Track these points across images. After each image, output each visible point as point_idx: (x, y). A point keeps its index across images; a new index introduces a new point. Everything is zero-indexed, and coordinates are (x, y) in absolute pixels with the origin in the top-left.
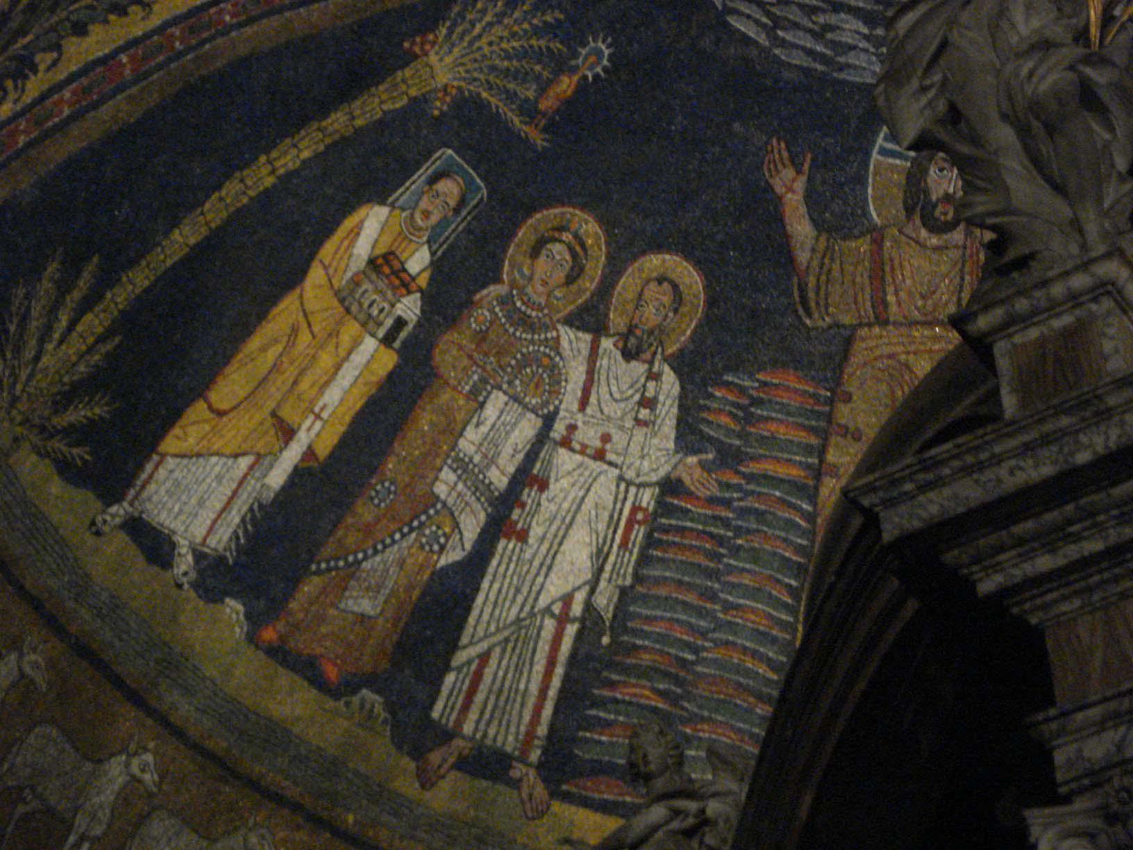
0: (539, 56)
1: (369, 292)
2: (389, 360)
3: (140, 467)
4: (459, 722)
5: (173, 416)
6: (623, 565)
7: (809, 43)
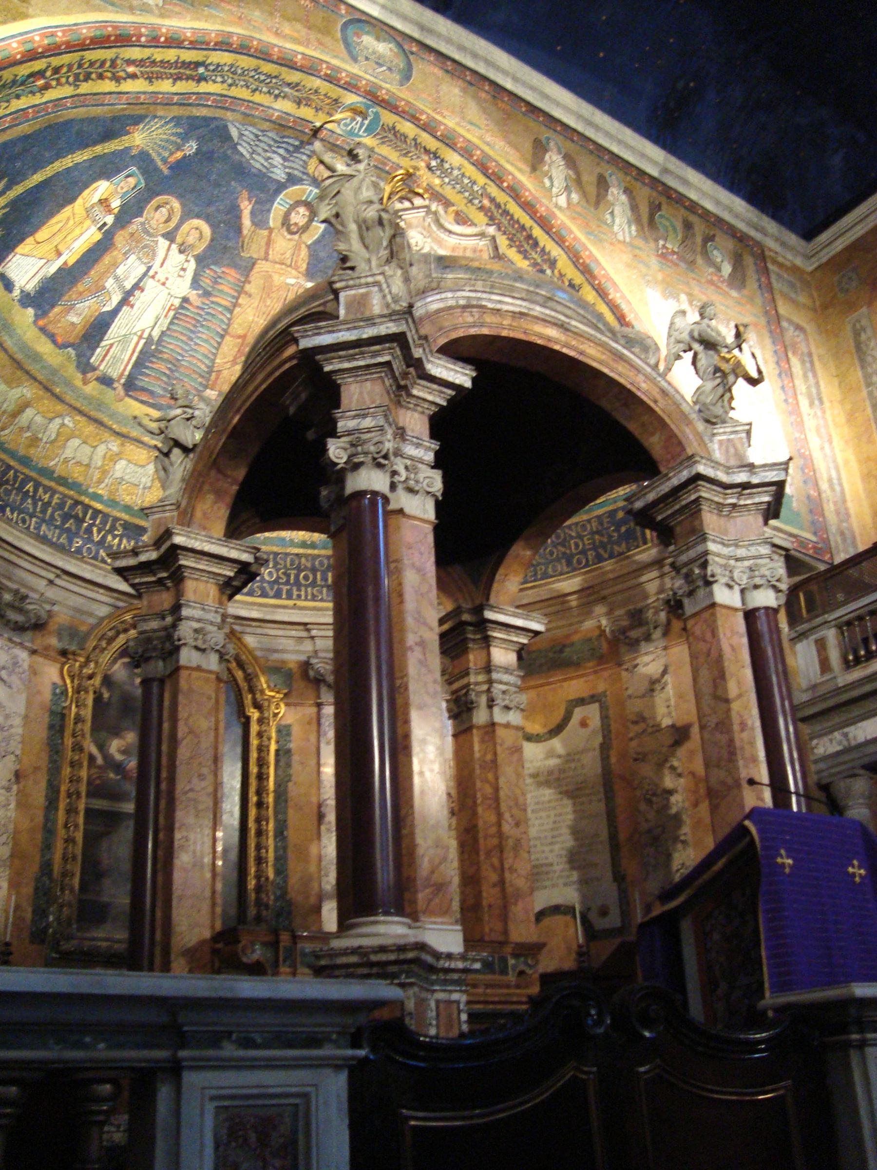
0: (173, 143)
2: (98, 236)
3: (7, 256)
5: (22, 240)
6: (164, 323)
7: (263, 161)
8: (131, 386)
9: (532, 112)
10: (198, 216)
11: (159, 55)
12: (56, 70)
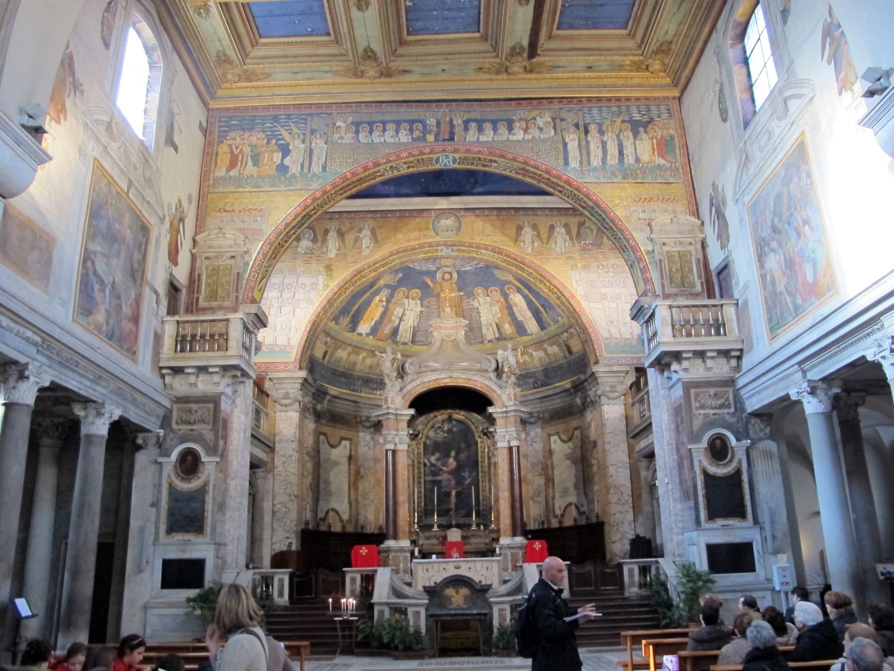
5: (359, 322)
6: (417, 321)
8: (413, 342)
9: (517, 212)
11: (374, 267)
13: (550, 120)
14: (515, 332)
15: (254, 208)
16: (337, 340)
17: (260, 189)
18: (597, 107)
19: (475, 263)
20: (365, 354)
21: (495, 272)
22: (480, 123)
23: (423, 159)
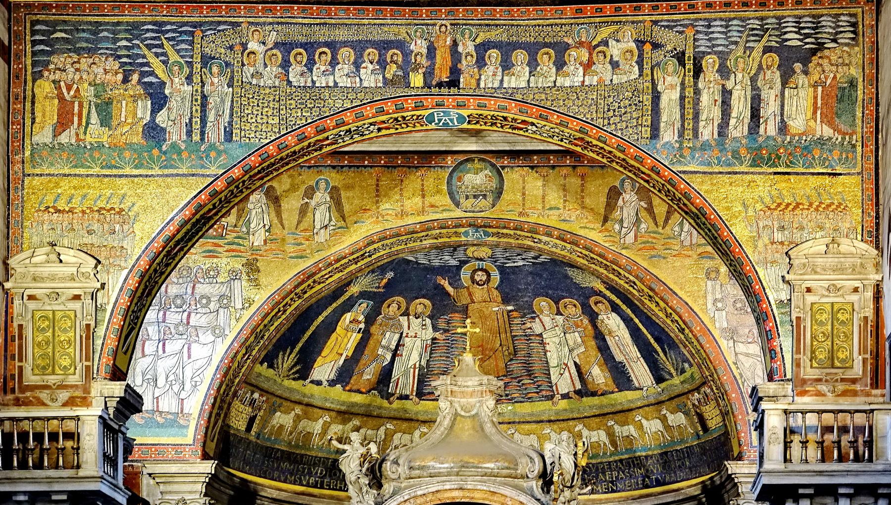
1: (352, 326)
2: (360, 335)
4: (395, 391)
10: (418, 298)
11: (338, 265)
12: (284, 306)
13: (633, 45)
14: (610, 382)
15: (109, 206)
16: (272, 394)
17: (115, 172)
18: (721, 19)
19: (532, 254)
20: (327, 418)
21: (570, 272)
22: (507, 49)
23: (404, 118)
